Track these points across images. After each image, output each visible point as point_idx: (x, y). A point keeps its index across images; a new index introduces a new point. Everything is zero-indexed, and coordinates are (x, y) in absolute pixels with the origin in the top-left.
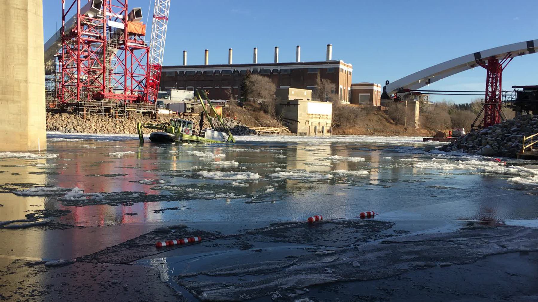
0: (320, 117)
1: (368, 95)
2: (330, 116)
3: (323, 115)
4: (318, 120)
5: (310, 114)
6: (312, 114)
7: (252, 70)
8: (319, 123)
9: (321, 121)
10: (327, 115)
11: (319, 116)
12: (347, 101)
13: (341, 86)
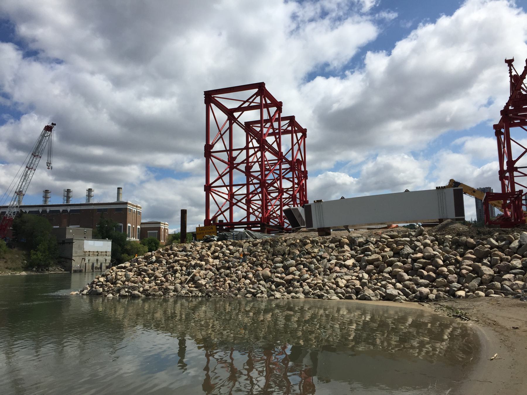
0: (98, 253)
1: (156, 233)
2: (110, 254)
3: (101, 252)
4: (96, 258)
5: (86, 252)
6: (89, 252)
7: (41, 211)
8: (97, 260)
10: (106, 252)
12: (136, 238)
13: (129, 225)
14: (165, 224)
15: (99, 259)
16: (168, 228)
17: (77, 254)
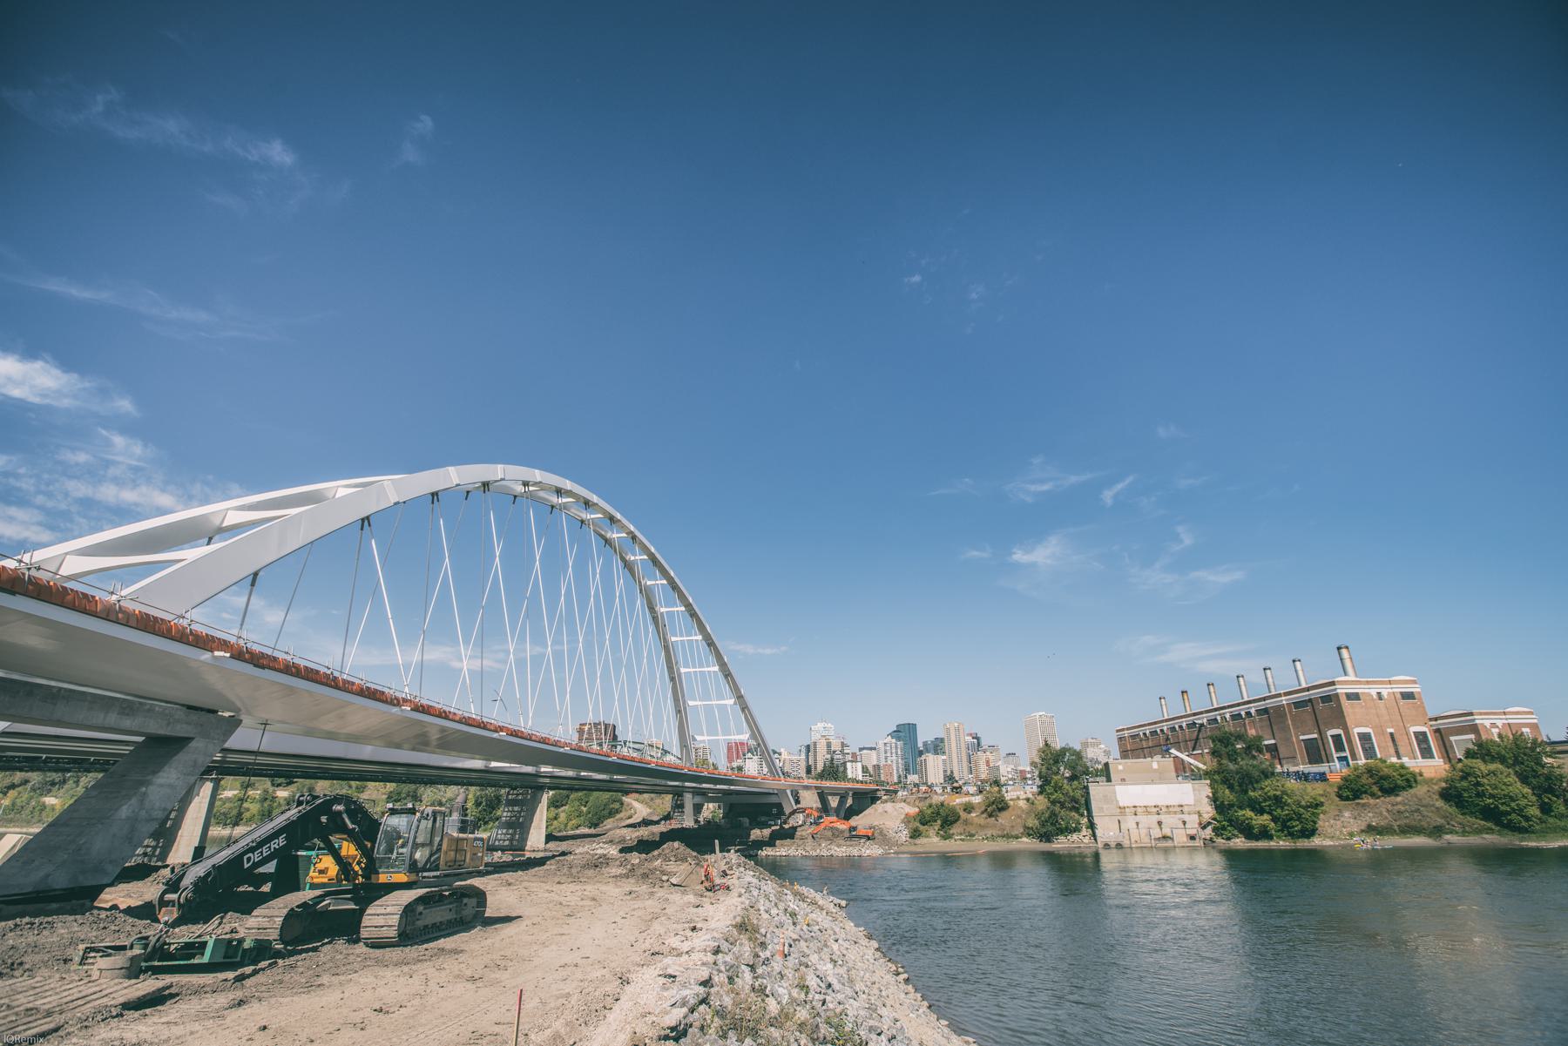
3: (1167, 807)
4: (1155, 818)
6: (1135, 807)
8: (1160, 823)
9: (1162, 818)
10: (1182, 806)
11: (1155, 810)
14: (1505, 713)
15: (1163, 821)
16: (1535, 721)
17: (1103, 812)
